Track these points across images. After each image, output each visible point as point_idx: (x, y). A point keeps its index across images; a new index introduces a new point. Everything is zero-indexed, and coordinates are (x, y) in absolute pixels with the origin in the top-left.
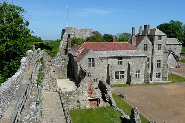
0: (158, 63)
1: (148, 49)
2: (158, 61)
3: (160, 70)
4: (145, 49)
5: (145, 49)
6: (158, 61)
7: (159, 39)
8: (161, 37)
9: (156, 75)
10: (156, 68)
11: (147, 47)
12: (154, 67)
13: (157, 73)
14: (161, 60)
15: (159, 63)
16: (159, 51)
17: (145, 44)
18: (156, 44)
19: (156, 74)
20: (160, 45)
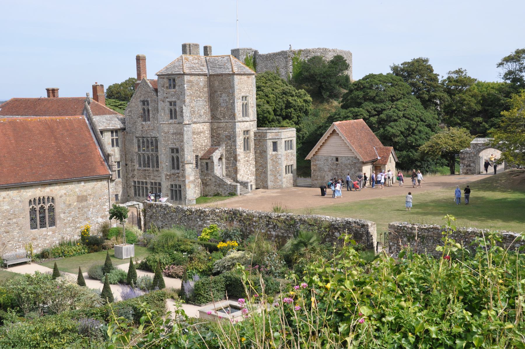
0: (173, 158)
1: (151, 115)
2: (172, 150)
3: (178, 177)
4: (145, 115)
5: (145, 115)
6: (172, 150)
7: (169, 87)
8: (174, 80)
9: (172, 190)
10: (167, 170)
11: (148, 110)
12: (164, 165)
13: (172, 186)
14: (177, 146)
15: (175, 155)
16: (171, 121)
17: (144, 102)
18: (163, 101)
19: (169, 187)
20: (175, 102)
